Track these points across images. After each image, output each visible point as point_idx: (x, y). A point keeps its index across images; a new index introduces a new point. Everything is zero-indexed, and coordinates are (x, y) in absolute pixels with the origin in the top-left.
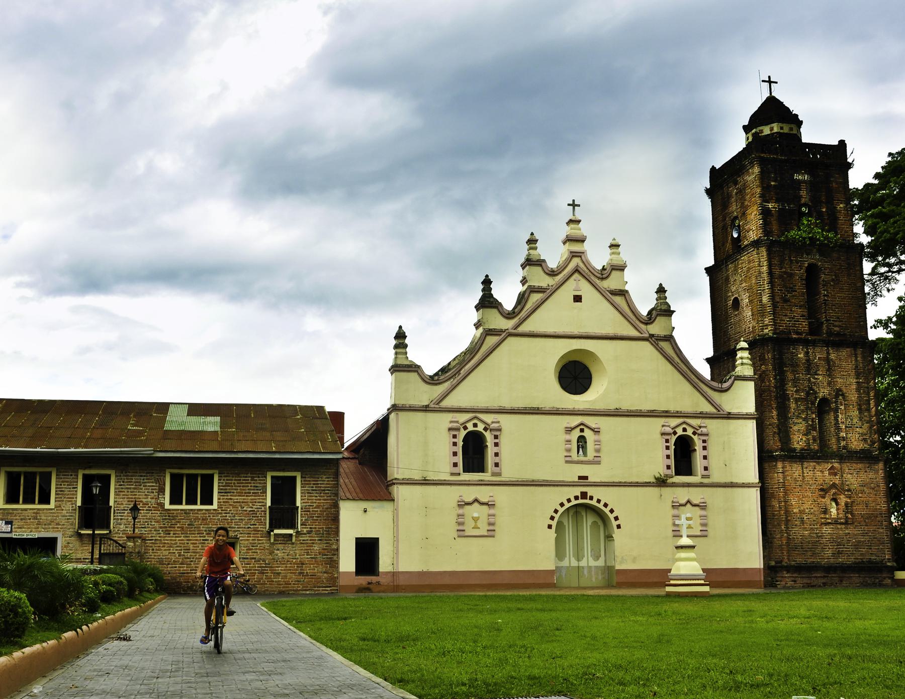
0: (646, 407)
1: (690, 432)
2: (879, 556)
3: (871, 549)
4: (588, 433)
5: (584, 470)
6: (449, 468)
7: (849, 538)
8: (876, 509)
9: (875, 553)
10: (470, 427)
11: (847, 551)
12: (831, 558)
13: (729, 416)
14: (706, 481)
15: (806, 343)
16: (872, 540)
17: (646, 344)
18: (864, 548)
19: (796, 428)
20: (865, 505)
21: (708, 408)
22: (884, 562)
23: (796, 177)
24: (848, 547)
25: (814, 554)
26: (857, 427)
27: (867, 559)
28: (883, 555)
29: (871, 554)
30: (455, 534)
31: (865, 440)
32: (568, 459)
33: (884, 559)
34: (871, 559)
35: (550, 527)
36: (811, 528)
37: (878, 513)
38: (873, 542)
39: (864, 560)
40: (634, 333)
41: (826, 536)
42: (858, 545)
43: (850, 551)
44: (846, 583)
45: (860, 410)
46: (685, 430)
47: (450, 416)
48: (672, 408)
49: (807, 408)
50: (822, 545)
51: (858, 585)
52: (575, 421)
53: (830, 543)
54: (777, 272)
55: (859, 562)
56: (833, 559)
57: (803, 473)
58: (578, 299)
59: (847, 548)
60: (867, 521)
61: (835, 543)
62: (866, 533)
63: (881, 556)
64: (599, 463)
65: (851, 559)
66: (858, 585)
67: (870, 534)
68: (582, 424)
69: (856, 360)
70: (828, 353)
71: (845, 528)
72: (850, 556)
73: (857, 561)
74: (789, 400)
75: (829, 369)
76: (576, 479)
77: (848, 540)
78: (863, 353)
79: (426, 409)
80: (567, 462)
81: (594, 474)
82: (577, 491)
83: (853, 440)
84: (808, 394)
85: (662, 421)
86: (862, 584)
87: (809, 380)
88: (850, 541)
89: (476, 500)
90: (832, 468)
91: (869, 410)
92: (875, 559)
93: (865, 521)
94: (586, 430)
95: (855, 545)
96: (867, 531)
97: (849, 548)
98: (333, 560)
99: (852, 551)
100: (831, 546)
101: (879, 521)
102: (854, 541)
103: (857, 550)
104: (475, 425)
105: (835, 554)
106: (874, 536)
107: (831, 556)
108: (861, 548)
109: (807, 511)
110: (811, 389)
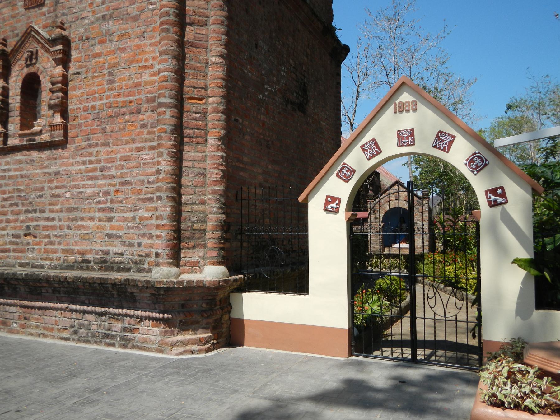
2: (131, 245)
3: (110, 220)
7: (57, 188)
8: (138, 85)
9: (121, 233)
11: (46, 228)
12: (8, 251)
16: (117, 191)
18: (91, 219)
20: (107, 77)
22: (146, 266)
24: (52, 215)
27: (97, 253)
28: (147, 241)
29: (110, 236)
33: (148, 255)
34: (107, 253)
37: (143, 97)
38: (120, 197)
39: (90, 257)
41: (7, 185)
42: (77, 209)
43: (53, 227)
44: (37, 327)
51: (65, 334)
53: (11, 205)
55: (76, 262)
56: (14, 250)
59: (47, 219)
60: (108, 128)
61: (23, 205)
62: (102, 170)
63: (139, 245)
65: (55, 252)
66: (65, 334)
67: (113, 172)
71: (48, 159)
72: (52, 243)
73: (71, 258)
77: (53, 196)
86: (75, 332)
88: (58, 196)
92: (122, 254)
93: (104, 131)
95: (70, 210)
96: (108, 161)
97: (53, 219)
99: (61, 228)
100: (12, 212)
101: (143, 126)
102: (68, 195)
103: (71, 224)
105: (18, 236)
106: (122, 176)
107: (11, 243)
108: (82, 219)
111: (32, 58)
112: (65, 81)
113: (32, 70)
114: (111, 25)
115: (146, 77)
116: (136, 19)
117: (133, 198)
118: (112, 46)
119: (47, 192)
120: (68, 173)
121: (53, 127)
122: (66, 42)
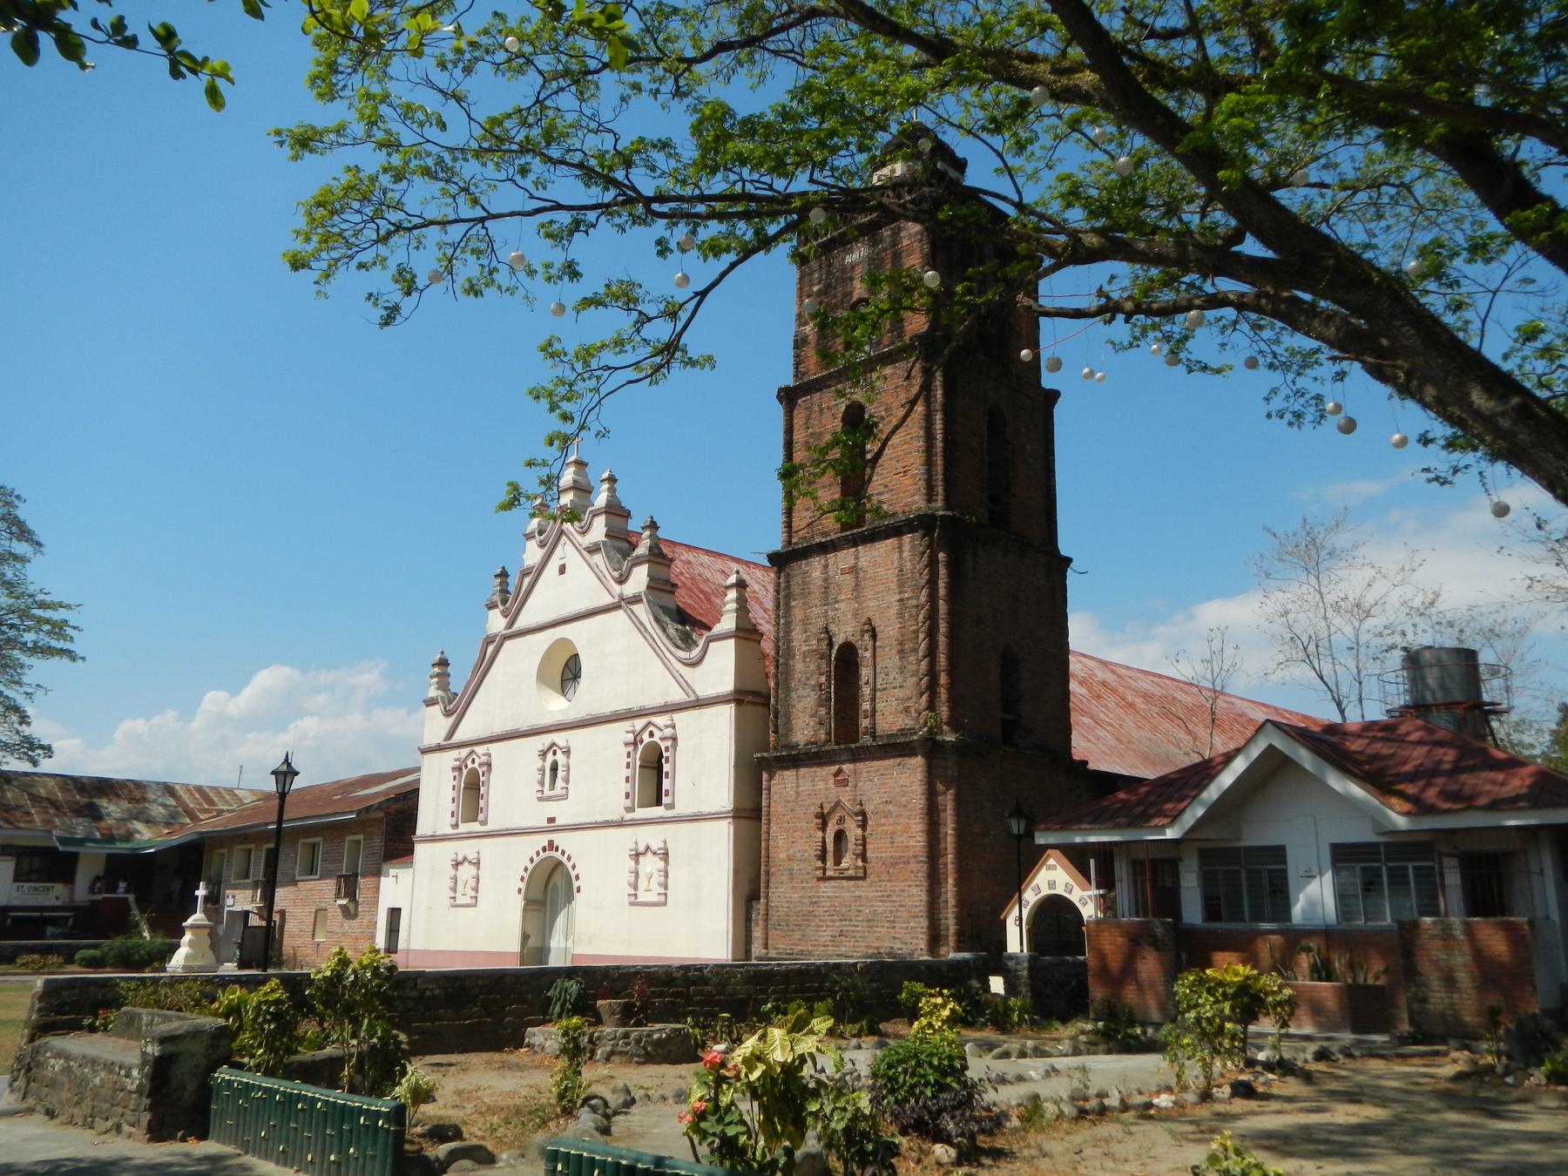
0: (607, 709)
1: (656, 739)
4: (560, 758)
5: (552, 809)
6: (449, 820)
10: (470, 765)
13: (699, 704)
14: (670, 813)
15: (824, 549)
17: (620, 613)
19: (800, 706)
21: (678, 696)
23: (848, 259)
25: (803, 938)
26: (895, 688)
28: (915, 941)
30: (448, 902)
31: (907, 710)
32: (540, 795)
35: (520, 891)
36: (803, 888)
37: (911, 854)
40: (607, 600)
45: (901, 652)
46: (651, 735)
47: (454, 754)
48: (635, 703)
49: (819, 668)
50: (817, 920)
52: (546, 740)
54: (799, 436)
57: (798, 786)
58: (562, 570)
64: (565, 797)
68: (553, 744)
69: (901, 557)
70: (857, 558)
73: (871, 951)
74: (794, 655)
75: (857, 585)
76: (546, 824)
78: (913, 540)
79: (439, 748)
80: (540, 799)
81: (565, 813)
82: (543, 840)
83: (887, 713)
84: (819, 640)
85: (626, 725)
87: (826, 614)
89: (465, 859)
90: (840, 772)
91: (915, 650)
94: (559, 752)
95: (869, 921)
98: (372, 937)
104: (473, 761)
109: (798, 855)
110: (826, 630)
111: (841, 820)
112: (864, 839)
113: (841, 827)
114: (890, 807)
115: (912, 843)
116: (906, 806)
117: (906, 915)
118: (892, 821)
119: (854, 908)
120: (867, 897)
121: (857, 868)
122: (863, 814)
